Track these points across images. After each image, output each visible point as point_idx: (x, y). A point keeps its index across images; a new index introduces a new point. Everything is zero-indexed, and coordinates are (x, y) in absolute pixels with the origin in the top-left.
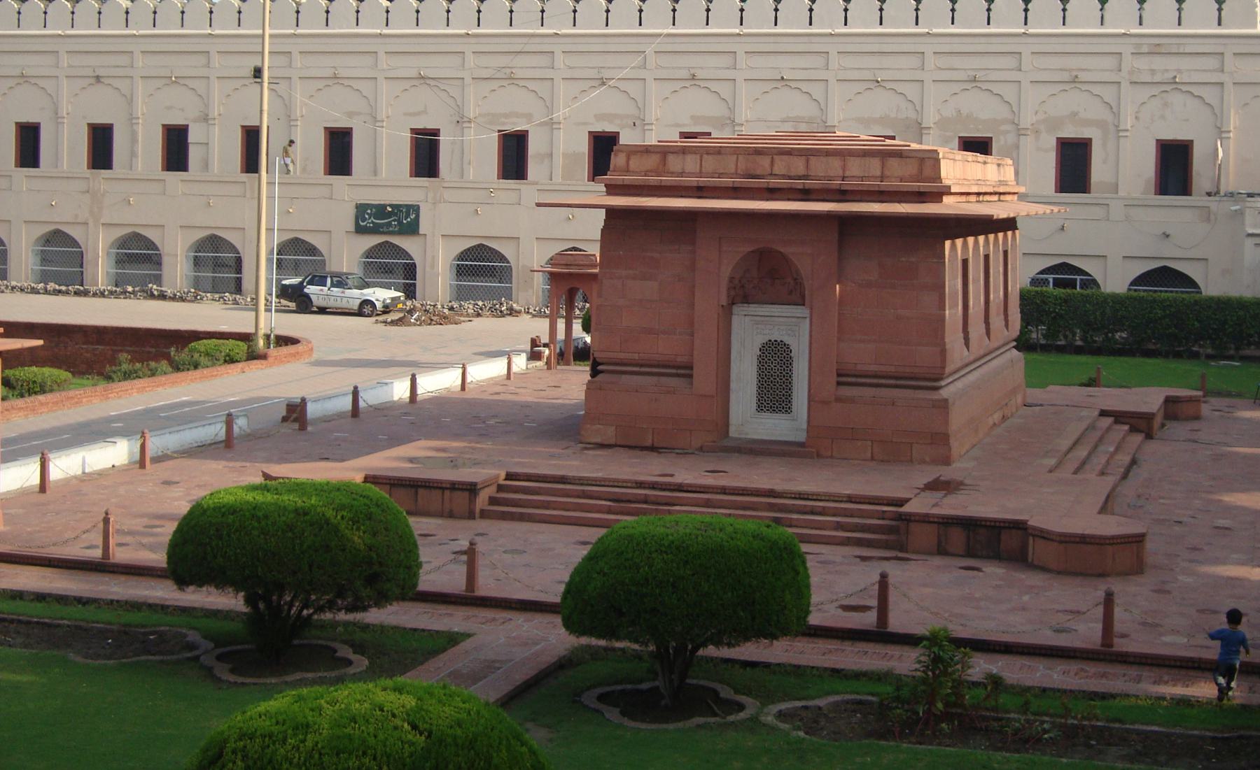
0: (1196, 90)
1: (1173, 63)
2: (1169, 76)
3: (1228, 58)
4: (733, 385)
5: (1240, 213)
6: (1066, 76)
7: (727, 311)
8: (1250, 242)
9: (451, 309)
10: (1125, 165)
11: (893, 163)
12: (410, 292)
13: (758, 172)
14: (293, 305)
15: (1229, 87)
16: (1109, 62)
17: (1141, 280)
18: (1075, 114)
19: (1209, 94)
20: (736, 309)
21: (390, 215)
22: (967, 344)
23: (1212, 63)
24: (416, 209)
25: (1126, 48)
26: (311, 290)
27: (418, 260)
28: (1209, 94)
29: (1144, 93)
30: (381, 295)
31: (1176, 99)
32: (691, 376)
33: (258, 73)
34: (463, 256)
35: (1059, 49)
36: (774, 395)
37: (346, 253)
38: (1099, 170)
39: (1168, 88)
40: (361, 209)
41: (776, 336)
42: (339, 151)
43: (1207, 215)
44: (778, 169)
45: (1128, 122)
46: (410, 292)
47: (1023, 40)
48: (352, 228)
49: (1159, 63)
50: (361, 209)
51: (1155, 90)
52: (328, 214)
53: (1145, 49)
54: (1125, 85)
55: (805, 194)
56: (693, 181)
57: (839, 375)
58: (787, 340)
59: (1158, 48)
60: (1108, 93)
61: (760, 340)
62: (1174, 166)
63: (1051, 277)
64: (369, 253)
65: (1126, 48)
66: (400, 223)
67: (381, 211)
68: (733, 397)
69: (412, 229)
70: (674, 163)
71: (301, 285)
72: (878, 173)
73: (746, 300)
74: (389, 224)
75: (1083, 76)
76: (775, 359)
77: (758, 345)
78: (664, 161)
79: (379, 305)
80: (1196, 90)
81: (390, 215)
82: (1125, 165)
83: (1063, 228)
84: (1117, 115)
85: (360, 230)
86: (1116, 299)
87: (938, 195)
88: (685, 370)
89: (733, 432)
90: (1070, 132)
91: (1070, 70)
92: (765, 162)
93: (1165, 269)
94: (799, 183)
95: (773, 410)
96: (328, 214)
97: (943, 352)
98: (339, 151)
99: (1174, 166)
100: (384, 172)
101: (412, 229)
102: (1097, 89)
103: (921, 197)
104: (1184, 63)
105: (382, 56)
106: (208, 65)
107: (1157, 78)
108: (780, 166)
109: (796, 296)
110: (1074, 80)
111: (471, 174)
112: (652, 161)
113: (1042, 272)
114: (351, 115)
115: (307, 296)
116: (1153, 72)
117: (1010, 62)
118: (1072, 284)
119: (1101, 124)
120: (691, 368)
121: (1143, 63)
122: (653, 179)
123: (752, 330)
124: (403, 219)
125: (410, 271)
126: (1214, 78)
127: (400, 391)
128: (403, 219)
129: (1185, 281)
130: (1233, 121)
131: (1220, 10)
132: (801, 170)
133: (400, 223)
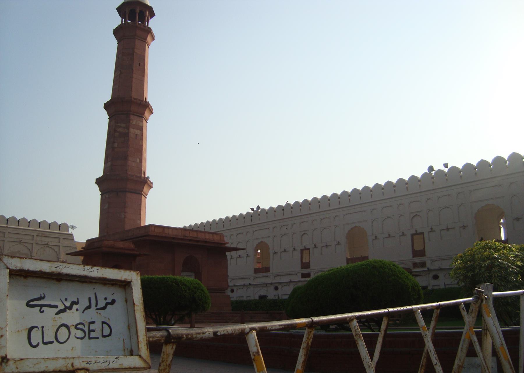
0: (53, 247)
1: (47, 240)
6: (17, 240)
11: (215, 235)
15: (61, 247)
16: (30, 237)
18: (19, 251)
19: (56, 249)
23: (57, 240)
35: (16, 232)
49: (43, 239)
51: (42, 246)
54: (34, 244)
60: (29, 246)
65: (35, 234)
87: (225, 244)
102: (27, 245)
107: (43, 243)
121: (39, 239)
126: (58, 244)
132: (196, 236)
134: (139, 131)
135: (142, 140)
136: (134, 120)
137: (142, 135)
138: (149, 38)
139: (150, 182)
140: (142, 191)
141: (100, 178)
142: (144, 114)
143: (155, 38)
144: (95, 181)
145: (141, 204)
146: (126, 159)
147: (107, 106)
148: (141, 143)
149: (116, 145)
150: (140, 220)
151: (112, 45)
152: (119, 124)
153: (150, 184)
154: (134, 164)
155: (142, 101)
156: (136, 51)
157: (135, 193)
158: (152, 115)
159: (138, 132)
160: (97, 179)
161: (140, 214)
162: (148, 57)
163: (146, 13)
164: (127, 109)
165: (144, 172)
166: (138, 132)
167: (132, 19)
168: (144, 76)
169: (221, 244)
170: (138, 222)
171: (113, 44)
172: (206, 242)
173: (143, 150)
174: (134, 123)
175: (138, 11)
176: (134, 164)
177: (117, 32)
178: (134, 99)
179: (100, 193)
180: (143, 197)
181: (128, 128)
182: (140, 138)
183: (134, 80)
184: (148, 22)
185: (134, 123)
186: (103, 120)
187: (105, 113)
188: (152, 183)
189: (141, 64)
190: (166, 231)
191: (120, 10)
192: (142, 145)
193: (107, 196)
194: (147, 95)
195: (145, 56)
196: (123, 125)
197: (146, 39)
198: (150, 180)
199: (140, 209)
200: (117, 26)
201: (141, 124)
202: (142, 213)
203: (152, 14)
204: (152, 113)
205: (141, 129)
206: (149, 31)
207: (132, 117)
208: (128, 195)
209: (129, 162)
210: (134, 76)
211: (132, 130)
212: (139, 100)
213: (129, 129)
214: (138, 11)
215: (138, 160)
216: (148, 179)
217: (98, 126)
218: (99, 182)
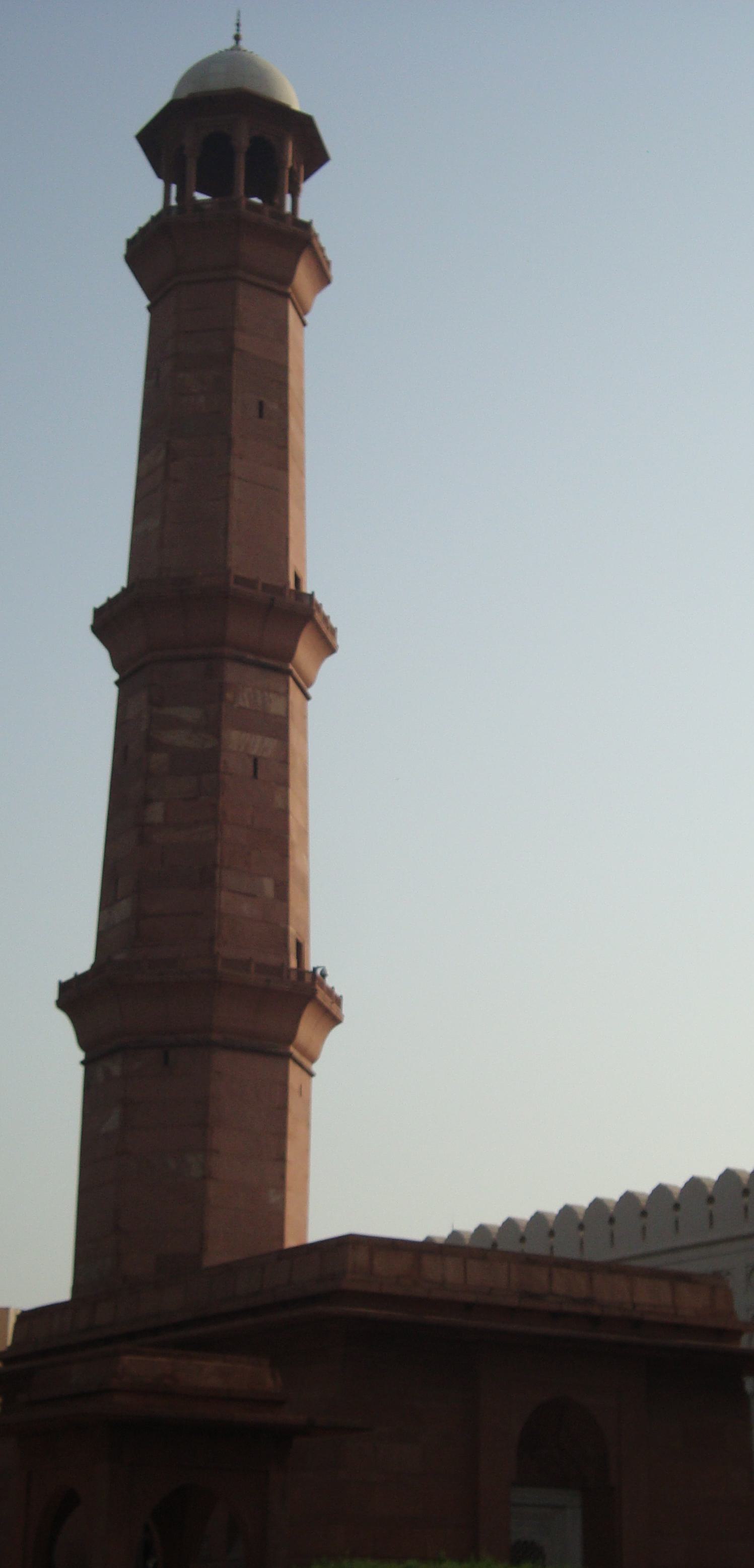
134: (271, 744)
136: (244, 687)
138: (303, 275)
139: (330, 992)
140: (290, 1037)
141: (79, 979)
143: (335, 272)
144: (54, 994)
147: (110, 623)
149: (156, 813)
151: (121, 322)
153: (328, 1003)
155: (282, 589)
158: (330, 663)
160: (64, 987)
162: (301, 372)
165: (300, 947)
167: (215, 178)
168: (284, 466)
169: (720, 1333)
170: (274, 1199)
173: (294, 836)
174: (244, 701)
175: (243, 140)
178: (239, 580)
179: (81, 1055)
181: (213, 727)
182: (273, 778)
184: (295, 192)
185: (244, 701)
186: (89, 691)
187: (100, 655)
188: (338, 1001)
191: (157, 140)
192: (285, 812)
193: (116, 1070)
194: (303, 560)
195: (284, 369)
197: (288, 279)
198: (329, 982)
200: (143, 220)
201: (275, 707)
203: (314, 155)
205: (279, 729)
206: (301, 239)
207: (233, 673)
211: (234, 738)
212: (265, 587)
213: (218, 736)
214: (243, 140)
215: (268, 886)
216: (317, 978)
218: (74, 997)
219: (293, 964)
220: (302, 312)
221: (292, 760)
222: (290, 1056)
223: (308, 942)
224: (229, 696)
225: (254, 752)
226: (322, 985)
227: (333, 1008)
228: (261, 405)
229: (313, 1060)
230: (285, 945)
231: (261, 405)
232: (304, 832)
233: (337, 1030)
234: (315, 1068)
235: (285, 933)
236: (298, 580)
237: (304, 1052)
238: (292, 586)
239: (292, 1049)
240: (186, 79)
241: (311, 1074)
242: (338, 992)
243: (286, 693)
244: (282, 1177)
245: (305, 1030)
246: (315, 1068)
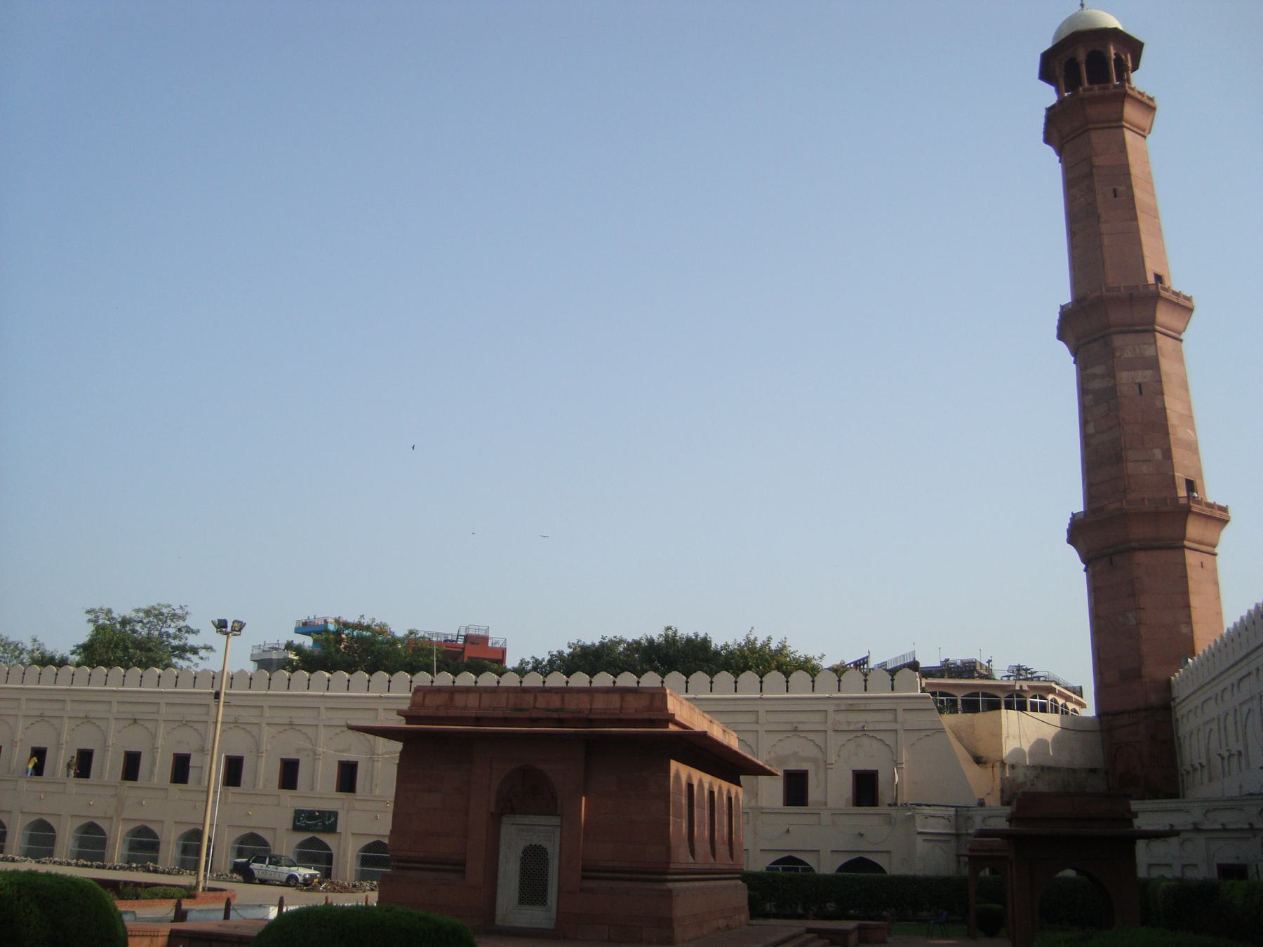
0: (878, 735)
2: (859, 726)
3: (900, 713)
4: (500, 881)
5: (912, 817)
6: (789, 727)
7: (496, 820)
8: (919, 839)
9: (354, 886)
10: (832, 788)
12: (327, 874)
13: (524, 706)
14: (240, 878)
15: (901, 733)
17: (845, 867)
18: (795, 753)
19: (888, 738)
20: (504, 819)
21: (315, 818)
22: (692, 852)
23: (889, 716)
24: (335, 814)
25: (830, 708)
26: (255, 866)
27: (334, 851)
28: (888, 738)
29: (843, 738)
30: (303, 872)
31: (865, 741)
32: (463, 872)
33: (217, 695)
34: (368, 848)
36: (532, 891)
37: (286, 842)
38: (813, 793)
39: (860, 734)
40: (298, 814)
41: (536, 841)
42: (289, 774)
43: (889, 820)
44: (538, 705)
45: (832, 758)
46: (327, 874)
47: (759, 702)
48: (290, 826)
49: (853, 717)
50: (298, 814)
51: (851, 736)
52: (272, 814)
53: (843, 708)
54: (830, 733)
55: (561, 722)
56: (473, 713)
57: (583, 870)
58: (544, 844)
59: (852, 706)
60: (818, 739)
61: (522, 845)
62: (866, 787)
63: (780, 867)
64: (303, 845)
65: (830, 708)
66: (324, 824)
67: (311, 815)
68: (500, 891)
69: (332, 829)
70: (460, 700)
71: (248, 863)
72: (618, 706)
73: (513, 811)
74: (316, 825)
75: (801, 727)
76: (534, 859)
77: (521, 848)
78: (452, 698)
79: (300, 879)
80: (878, 735)
81: (315, 818)
82: (832, 788)
83: (788, 831)
84: (825, 753)
85: (296, 828)
86: (826, 879)
88: (459, 866)
89: (499, 921)
90: (793, 766)
91: (791, 723)
92: (529, 698)
93: (861, 859)
94: (555, 715)
95: (532, 902)
96: (272, 814)
97: (668, 848)
98: (289, 774)
99: (866, 787)
100: (317, 788)
101: (332, 829)
102: (811, 736)
103: (652, 723)
104: (870, 717)
105: (323, 711)
106: (208, 714)
108: (541, 702)
109: (550, 808)
110: (795, 730)
111: (377, 792)
112: (440, 699)
113: (774, 863)
114: (298, 750)
115: (251, 872)
116: (849, 723)
117: (752, 718)
118: (797, 870)
119: (814, 760)
120: (464, 865)
121: (841, 717)
122: (442, 713)
123: (515, 838)
124: (325, 821)
125: (329, 859)
126: (893, 726)
127: (273, 913)
128: (325, 821)
129: (877, 868)
130: (905, 756)
131: (892, 680)
133: (324, 824)
134: (1149, 373)
135: (1162, 393)
136: (1126, 346)
137: (1160, 381)
140: (1183, 538)
142: (1153, 321)
143: (1158, 103)
145: (1184, 577)
146: (1119, 459)
148: (1159, 405)
150: (1189, 622)
152: (1089, 371)
153: (1207, 511)
154: (1145, 469)
156: (1097, 161)
157: (1159, 548)
159: (1143, 376)
161: (1187, 606)
163: (1108, 51)
164: (1115, 320)
165: (1191, 486)
166: (1143, 376)
168: (1135, 218)
169: (652, 723)
170: (1184, 629)
171: (1049, 165)
172: (590, 722)
174: (1128, 354)
175: (1082, 56)
176: (1145, 469)
177: (1061, 129)
180: (1192, 558)
181: (1111, 374)
183: (1106, 240)
186: (1061, 368)
189: (1121, 189)
190: (460, 700)
192: (1164, 409)
196: (1099, 370)
197: (1121, 118)
199: (1186, 593)
201: (1149, 352)
202: (1195, 601)
203: (1133, 48)
204: (1190, 310)
205: (1153, 364)
207: (1118, 341)
208: (1141, 557)
209: (1131, 467)
210: (1105, 228)
211: (1124, 376)
213: (1114, 378)
215: (1158, 454)
217: (1047, 394)
219: (1182, 492)
220: (1143, 132)
221: (1164, 378)
222: (1185, 547)
223: (1201, 478)
224: (1118, 354)
225: (1138, 381)
226: (1199, 502)
227: (1218, 514)
228: (1115, 191)
229: (1214, 546)
230: (1174, 483)
231: (1115, 191)
232: (1189, 419)
233: (1229, 525)
234: (1217, 550)
235: (1173, 476)
236: (1159, 278)
237: (1200, 543)
238: (1151, 280)
239: (1186, 543)
240: (1055, 38)
241: (1215, 555)
242: (1223, 504)
243: (1155, 341)
244: (1190, 617)
245: (1194, 529)
246: (1217, 550)
